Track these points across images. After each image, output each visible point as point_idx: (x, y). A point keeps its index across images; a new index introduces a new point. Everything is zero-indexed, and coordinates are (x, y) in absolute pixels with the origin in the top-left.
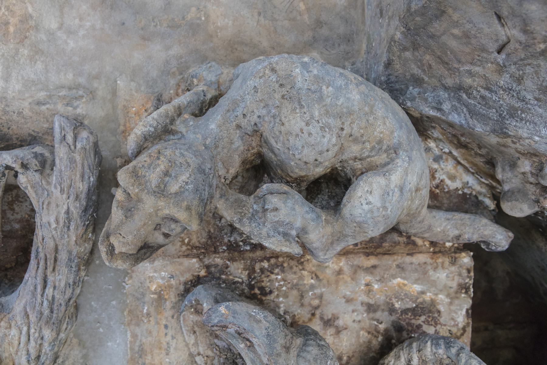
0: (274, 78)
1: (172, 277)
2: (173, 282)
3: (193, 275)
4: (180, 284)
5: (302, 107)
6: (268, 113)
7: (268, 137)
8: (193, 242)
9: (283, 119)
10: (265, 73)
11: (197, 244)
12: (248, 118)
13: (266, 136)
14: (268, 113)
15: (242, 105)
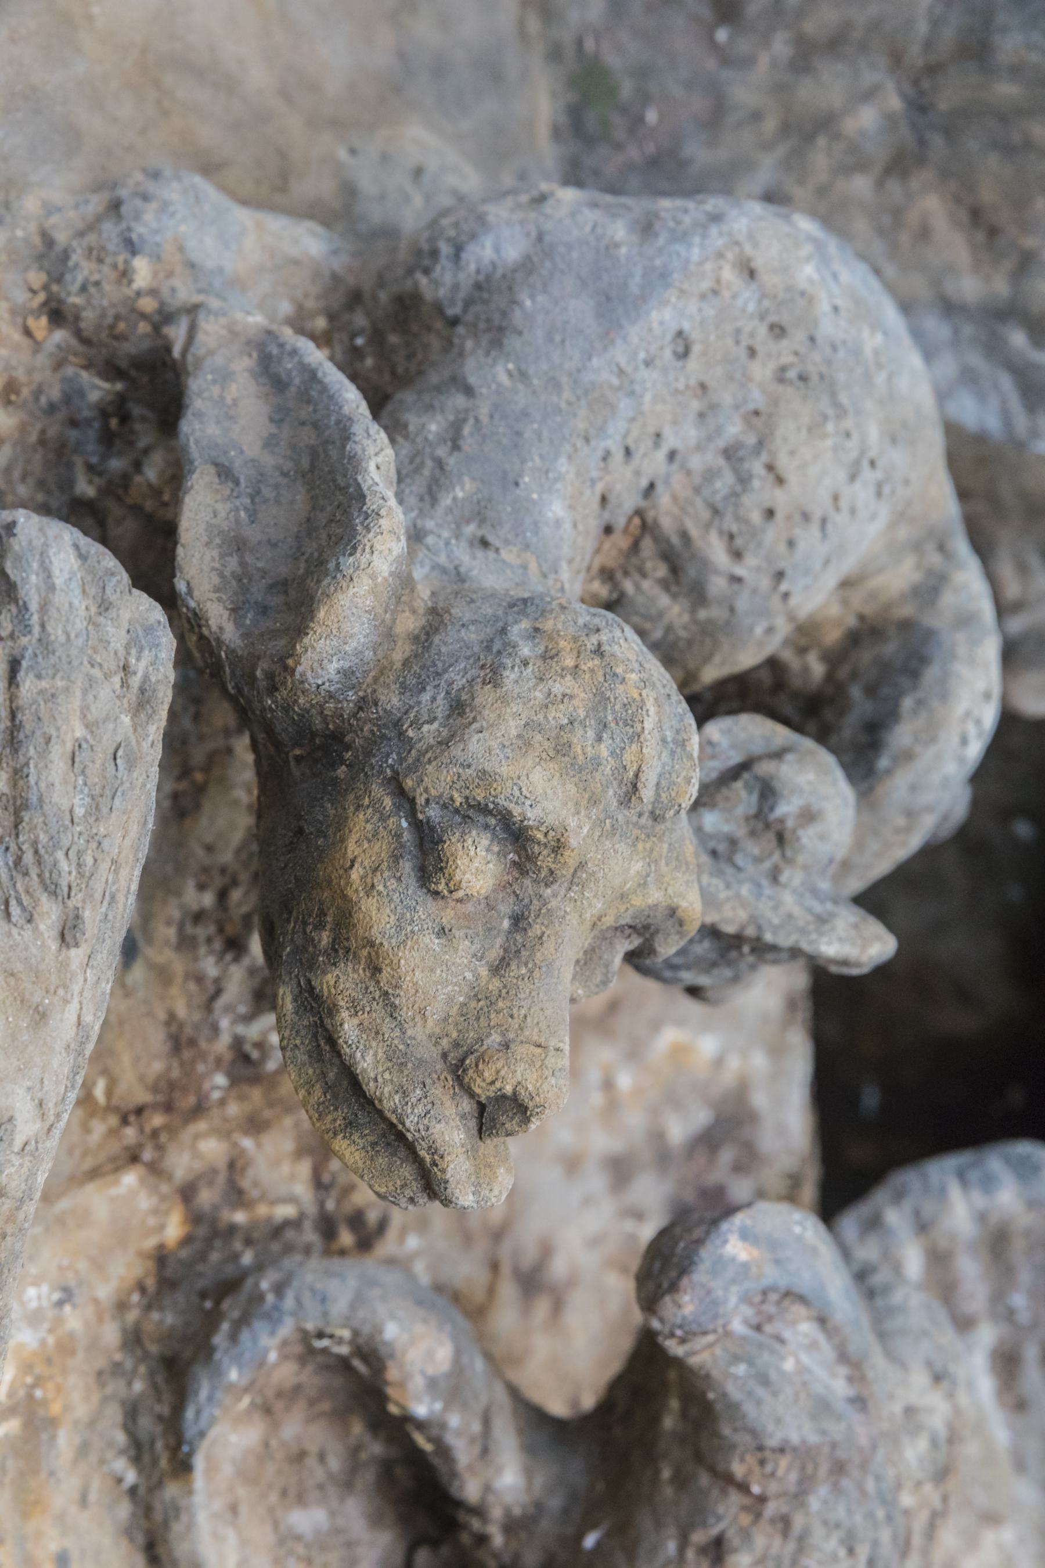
0: (748, 298)
1: (67, 1296)
2: (74, 1320)
3: (140, 1254)
4: (100, 1320)
5: (841, 412)
6: (710, 439)
7: (694, 532)
8: (122, 1087)
9: (784, 462)
10: (718, 281)
11: (142, 1096)
12: (636, 461)
13: (685, 535)
14: (710, 439)
15: (625, 406)
